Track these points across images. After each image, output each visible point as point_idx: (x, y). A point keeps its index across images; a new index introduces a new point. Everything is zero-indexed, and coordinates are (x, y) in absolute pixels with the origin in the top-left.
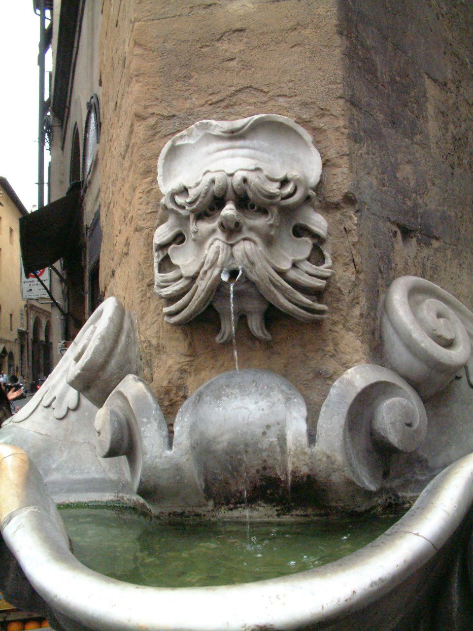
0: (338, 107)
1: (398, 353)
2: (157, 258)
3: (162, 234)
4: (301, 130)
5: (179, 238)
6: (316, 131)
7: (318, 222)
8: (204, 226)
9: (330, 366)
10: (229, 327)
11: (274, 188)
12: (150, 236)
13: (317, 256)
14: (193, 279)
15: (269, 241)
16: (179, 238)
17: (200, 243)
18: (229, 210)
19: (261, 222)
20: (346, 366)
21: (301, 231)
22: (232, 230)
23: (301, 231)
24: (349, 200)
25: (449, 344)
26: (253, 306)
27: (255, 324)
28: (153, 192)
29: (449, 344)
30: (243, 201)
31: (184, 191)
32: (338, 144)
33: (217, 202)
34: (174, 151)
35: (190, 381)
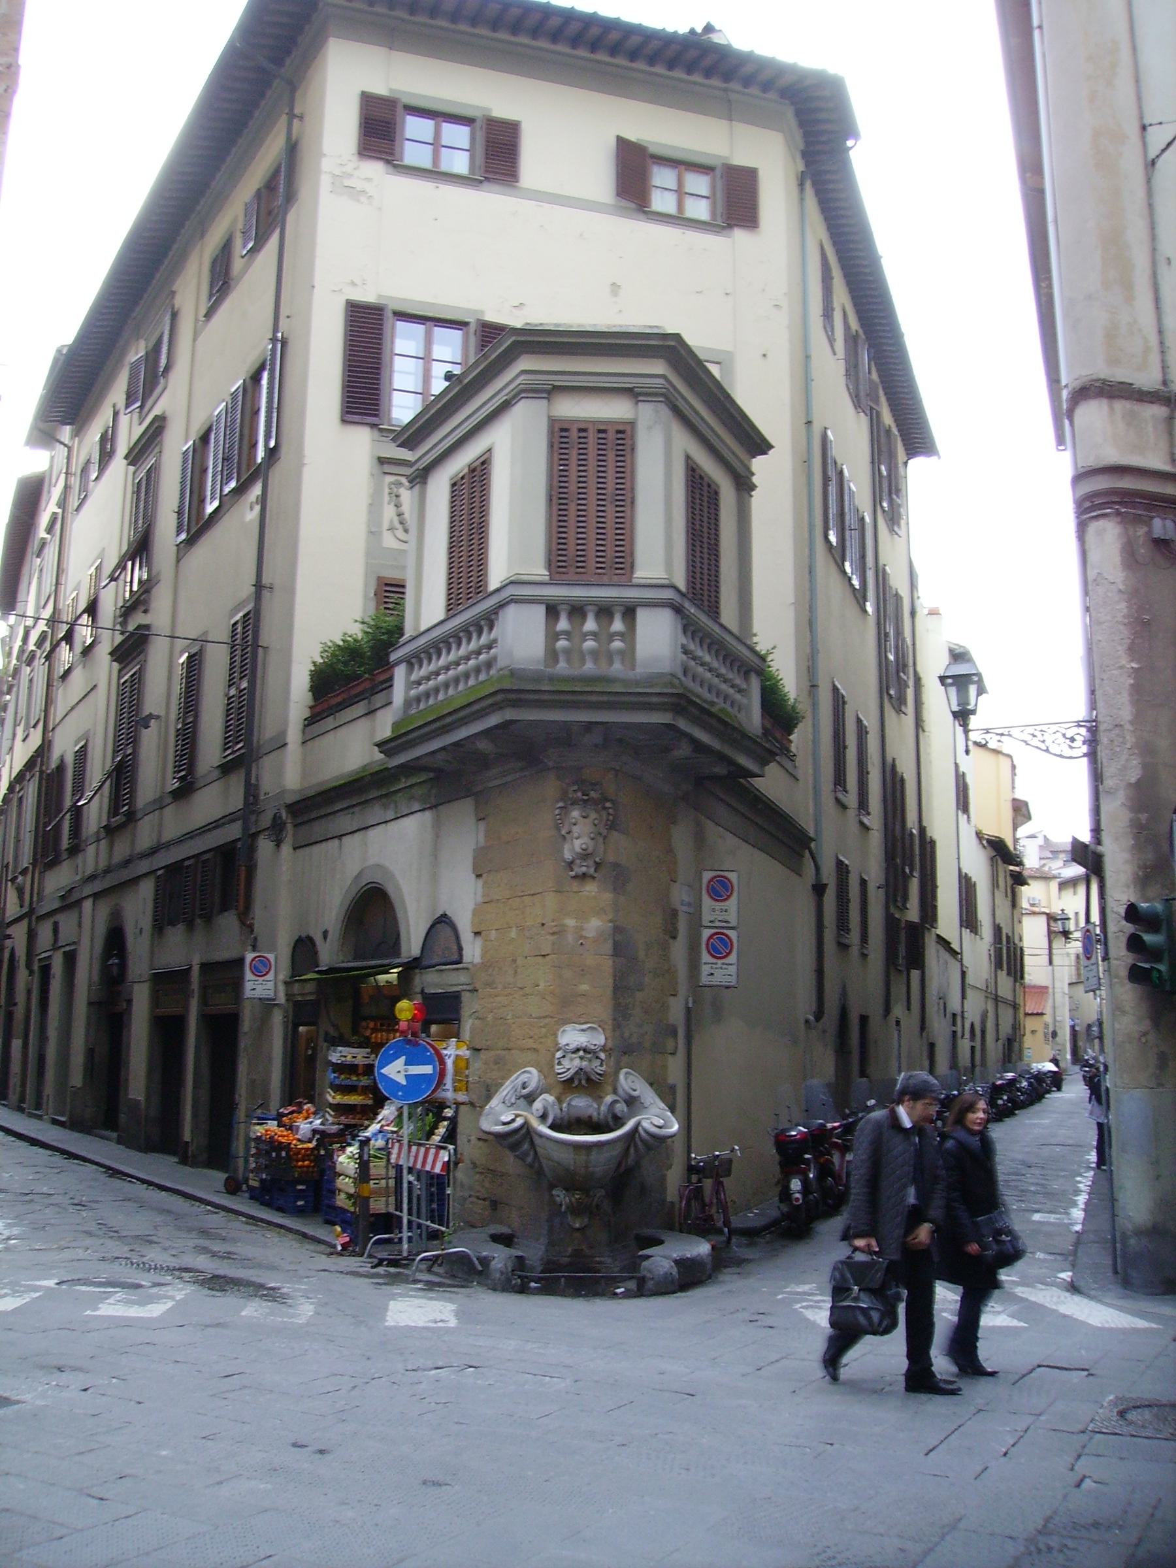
0: (610, 1022)
1: (620, 1091)
2: (556, 1061)
3: (559, 1054)
4: (600, 1029)
5: (564, 1057)
6: (603, 1029)
7: (602, 1056)
8: (574, 1056)
9: (602, 1095)
10: (576, 1082)
11: (593, 1047)
12: (554, 1056)
13: (601, 1065)
14: (569, 1069)
15: (590, 1060)
16: (564, 1057)
17: (572, 1060)
18: (581, 1053)
19: (589, 1056)
20: (607, 1094)
21: (597, 1058)
22: (581, 1058)
23: (597, 1058)
24: (611, 1049)
25: (635, 1090)
26: (583, 1076)
27: (583, 1082)
28: (557, 1044)
29: (635, 1090)
30: (585, 1050)
31: (567, 1045)
32: (609, 1033)
33: (578, 1050)
34: (564, 1031)
35: (563, 1097)
